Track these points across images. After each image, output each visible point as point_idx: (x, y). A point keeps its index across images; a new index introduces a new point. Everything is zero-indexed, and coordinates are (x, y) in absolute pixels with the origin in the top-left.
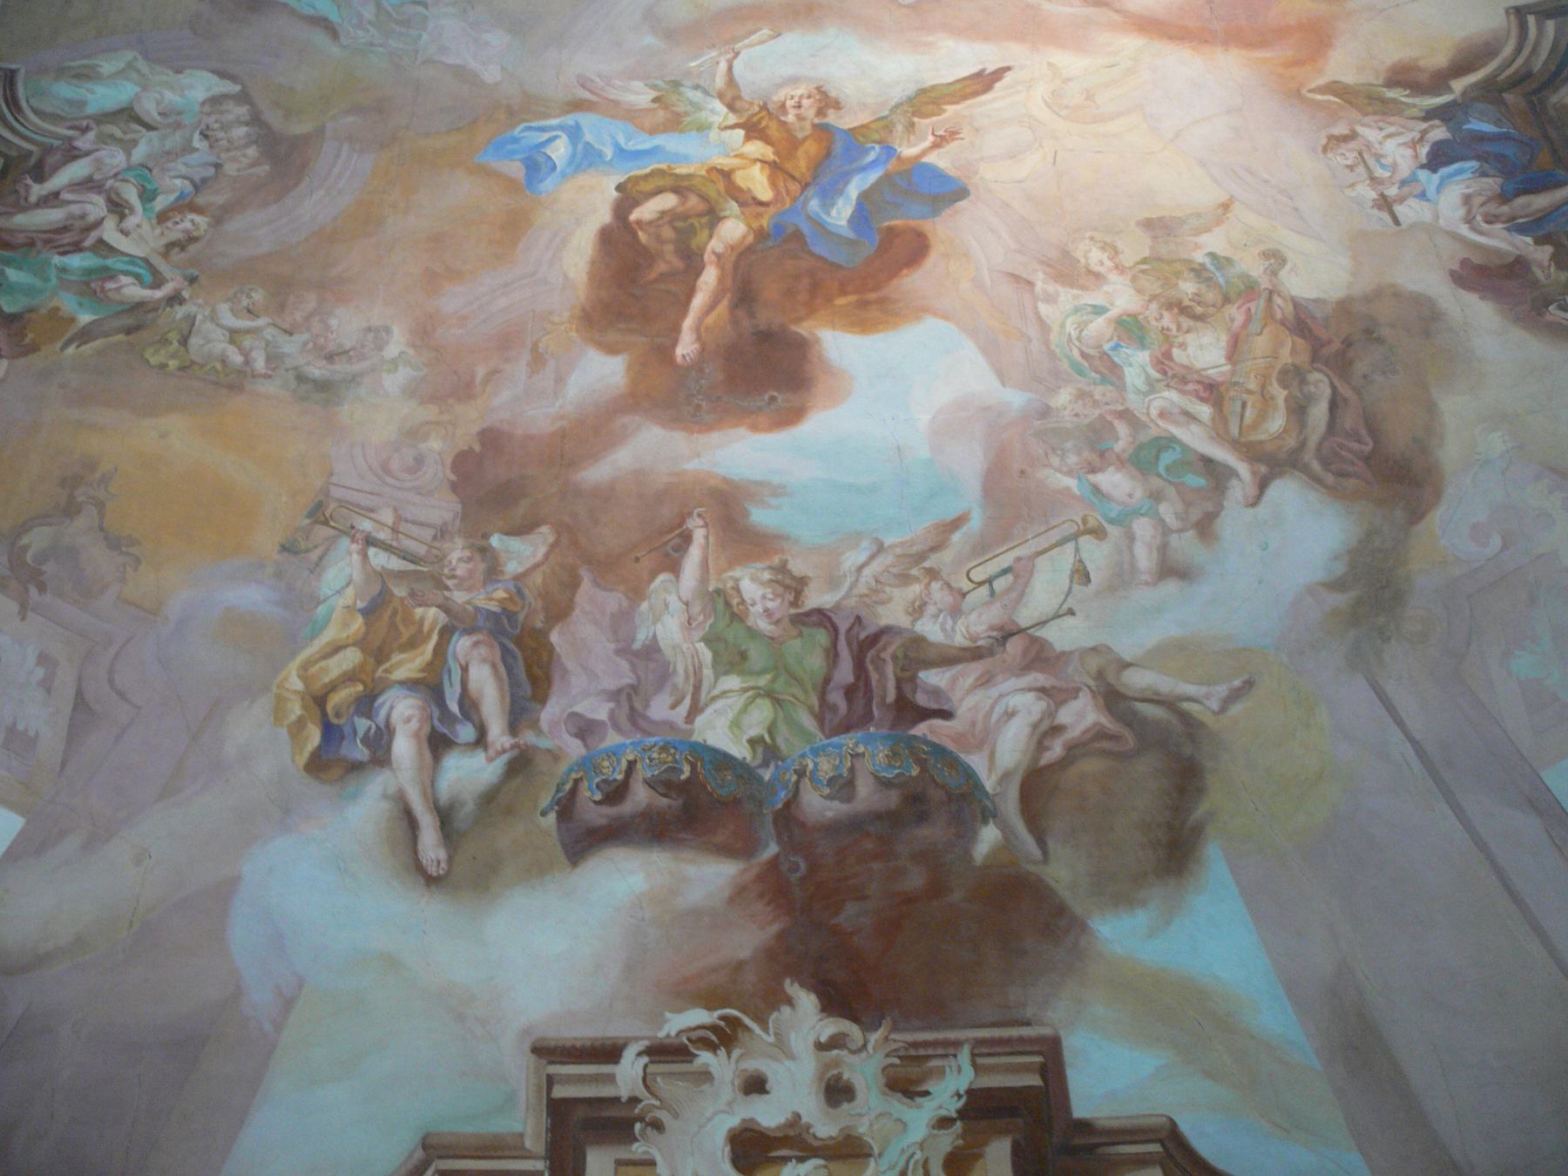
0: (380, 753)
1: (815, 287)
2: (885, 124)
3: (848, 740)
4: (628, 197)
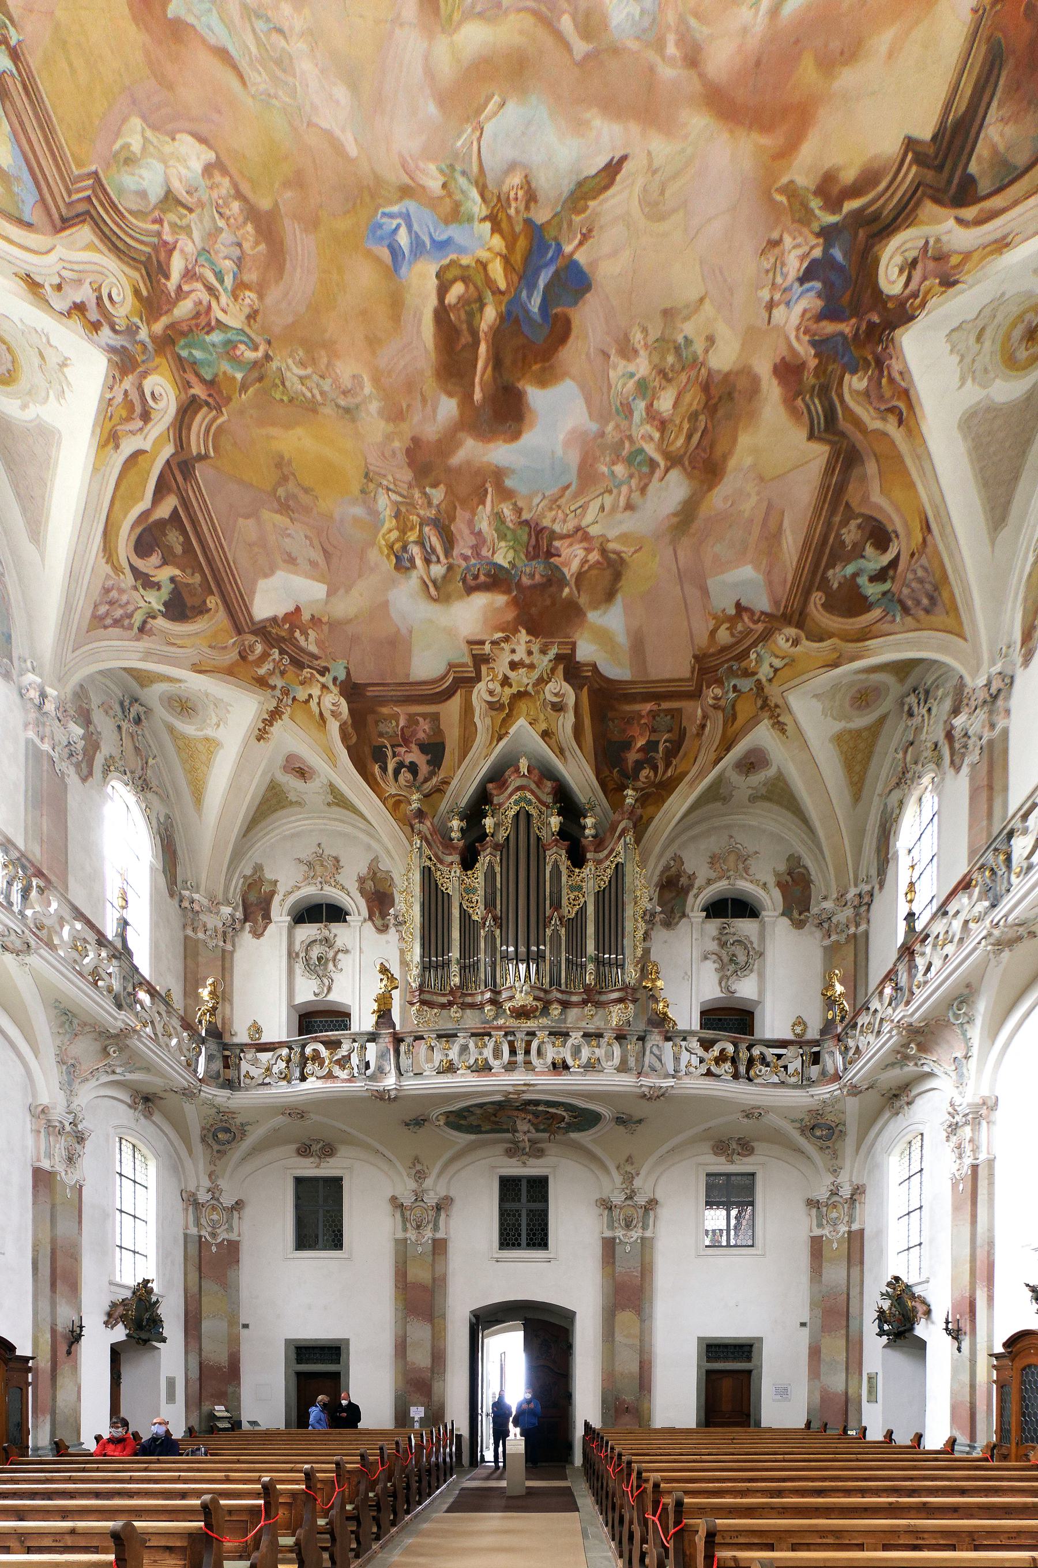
1: (524, 358)
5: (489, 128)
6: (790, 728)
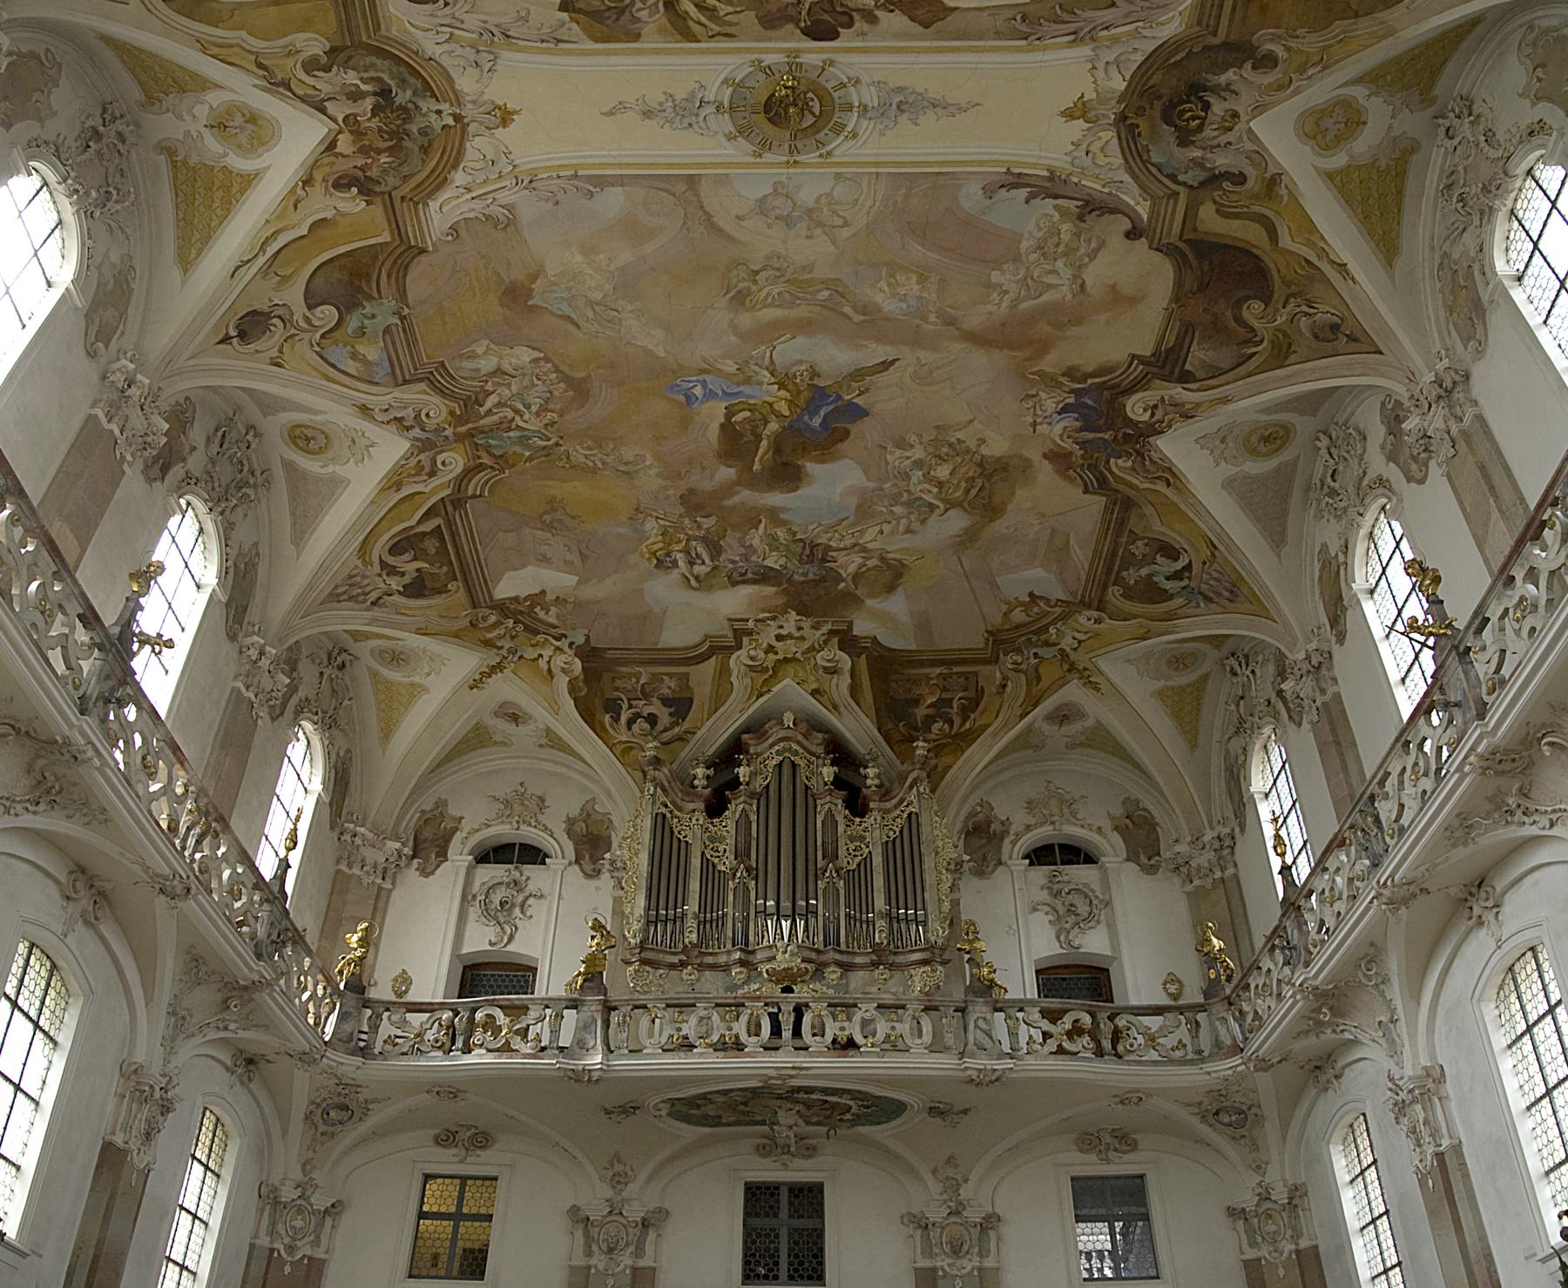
0: (675, 564)
1: (804, 448)
6: (1104, 686)
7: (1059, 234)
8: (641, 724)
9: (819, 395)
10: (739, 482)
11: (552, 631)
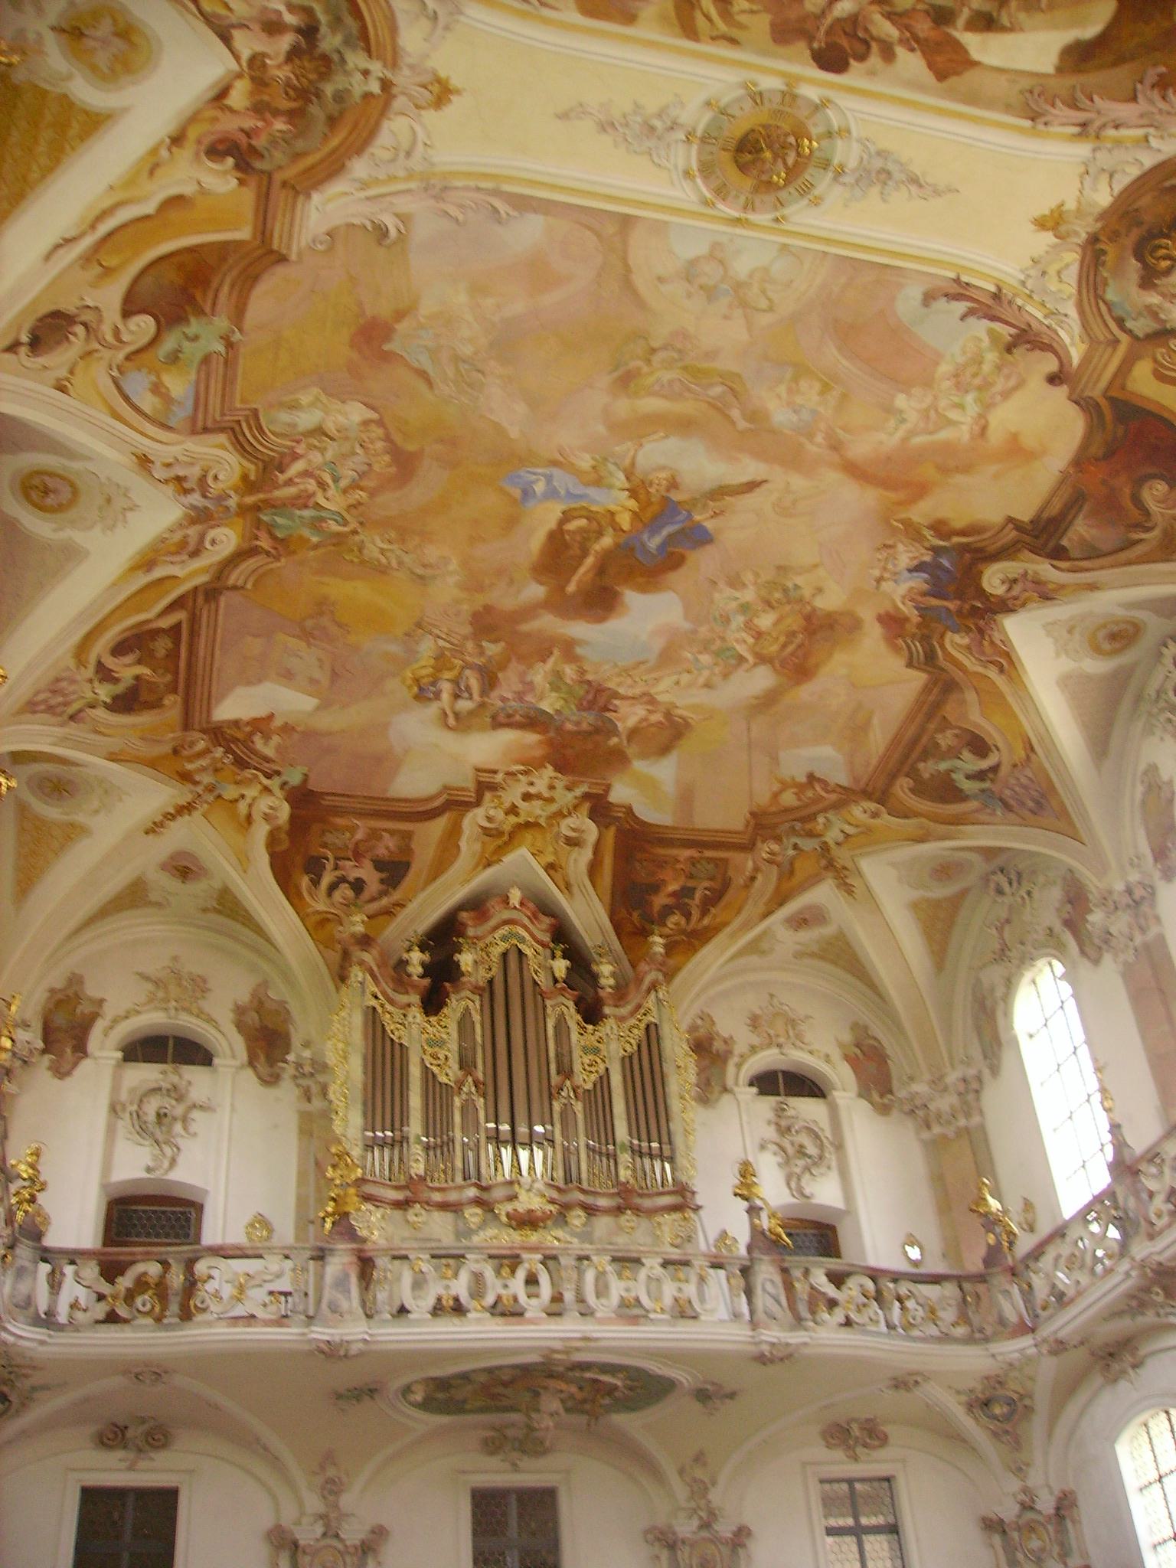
0: (437, 696)
2: (694, 502)
3: (584, 714)
4: (567, 516)
5: (648, 447)
6: (859, 891)
7: (980, 363)
8: (345, 892)
9: (668, 509)
10: (547, 605)
11: (266, 766)
